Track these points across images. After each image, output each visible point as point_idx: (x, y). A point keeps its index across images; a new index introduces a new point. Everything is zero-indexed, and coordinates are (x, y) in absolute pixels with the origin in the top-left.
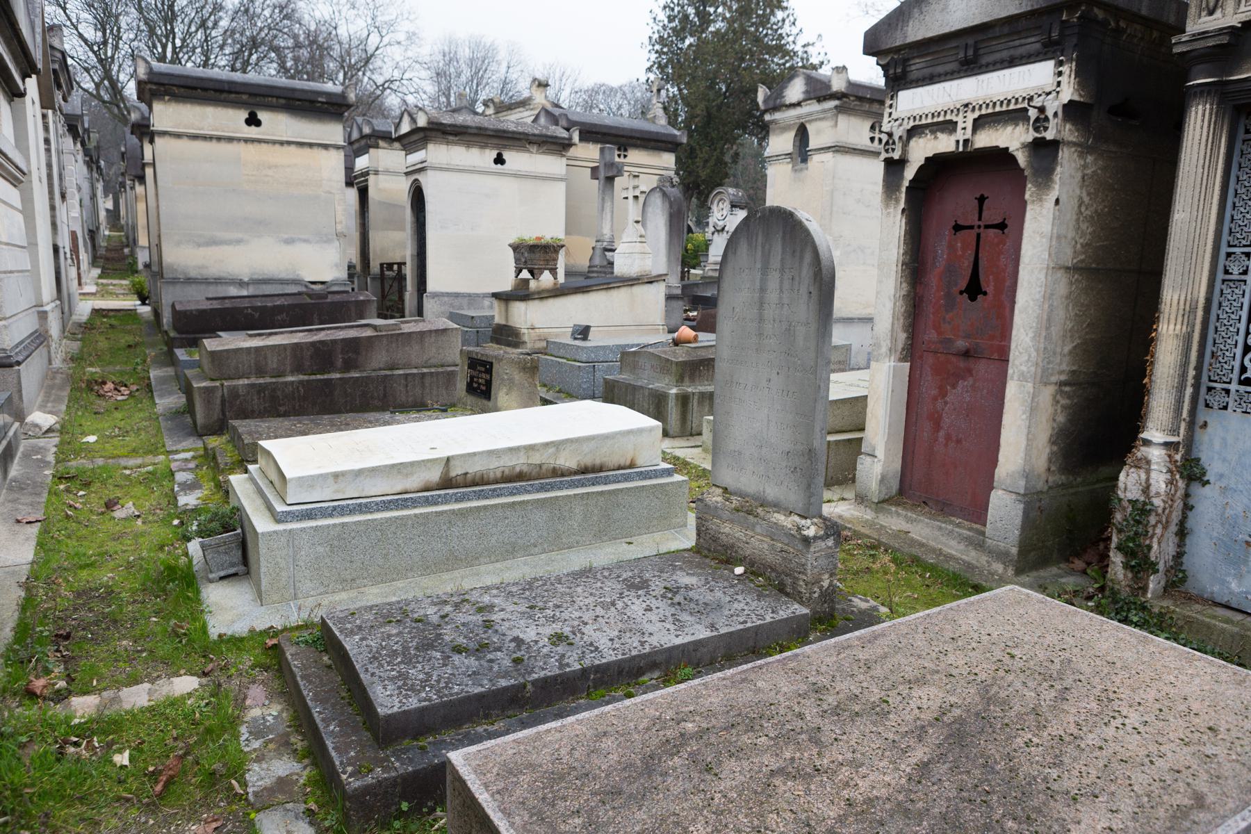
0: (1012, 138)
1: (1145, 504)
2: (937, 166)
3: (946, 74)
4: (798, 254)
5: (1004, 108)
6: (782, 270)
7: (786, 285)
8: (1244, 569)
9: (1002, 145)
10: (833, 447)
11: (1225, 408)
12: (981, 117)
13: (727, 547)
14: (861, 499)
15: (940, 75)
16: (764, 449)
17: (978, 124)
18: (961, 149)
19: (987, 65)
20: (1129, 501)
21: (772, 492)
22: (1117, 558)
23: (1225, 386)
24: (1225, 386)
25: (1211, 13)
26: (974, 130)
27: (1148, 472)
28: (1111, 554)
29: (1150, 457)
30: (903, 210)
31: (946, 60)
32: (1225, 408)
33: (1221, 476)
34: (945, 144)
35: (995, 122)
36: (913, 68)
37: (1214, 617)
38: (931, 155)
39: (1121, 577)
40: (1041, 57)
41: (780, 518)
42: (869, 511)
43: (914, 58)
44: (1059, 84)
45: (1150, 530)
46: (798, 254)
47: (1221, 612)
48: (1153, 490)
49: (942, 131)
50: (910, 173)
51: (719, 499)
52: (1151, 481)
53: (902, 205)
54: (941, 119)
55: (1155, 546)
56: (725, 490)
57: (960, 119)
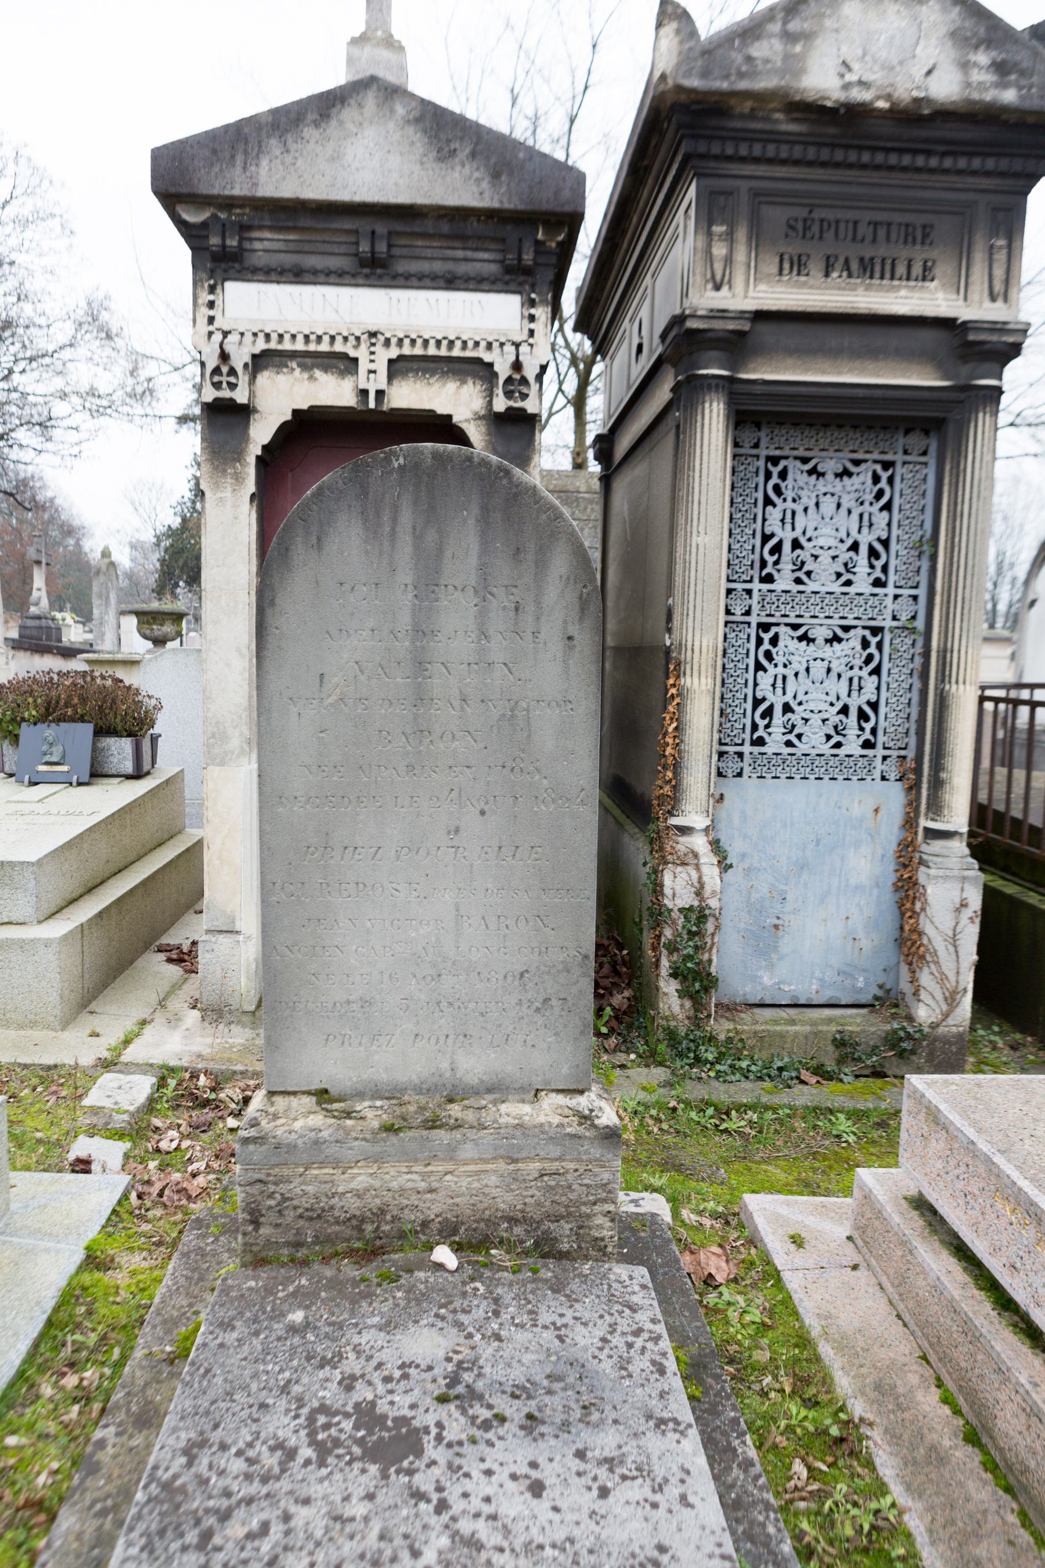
0: (459, 401)
1: (702, 909)
2: (308, 429)
3: (328, 273)
4: (530, 556)
5: (443, 352)
6: (483, 589)
7: (499, 621)
8: (774, 956)
9: (441, 410)
10: (86, 927)
11: (740, 775)
12: (401, 358)
13: (357, 1222)
14: (215, 1013)
15: (315, 272)
16: (448, 981)
17: (398, 367)
18: (372, 405)
19: (408, 277)
20: (681, 910)
21: (473, 1065)
22: (669, 988)
23: (738, 749)
24: (738, 749)
25: (717, 288)
26: (390, 378)
27: (697, 867)
28: (662, 984)
29: (696, 849)
30: (253, 496)
31: (329, 248)
32: (740, 775)
33: (744, 856)
34: (334, 392)
35: (425, 371)
36: (257, 245)
37: (776, 1022)
38: (305, 407)
40: (499, 285)
41: (513, 1111)
42: (236, 1029)
43: (261, 228)
44: (532, 333)
45: (708, 940)
46: (530, 556)
47: (768, 1013)
48: (707, 891)
49: (326, 369)
50: (261, 432)
51: (317, 1120)
52: (705, 879)
54: (324, 347)
55: (714, 958)
56: (322, 1095)
57: (362, 354)
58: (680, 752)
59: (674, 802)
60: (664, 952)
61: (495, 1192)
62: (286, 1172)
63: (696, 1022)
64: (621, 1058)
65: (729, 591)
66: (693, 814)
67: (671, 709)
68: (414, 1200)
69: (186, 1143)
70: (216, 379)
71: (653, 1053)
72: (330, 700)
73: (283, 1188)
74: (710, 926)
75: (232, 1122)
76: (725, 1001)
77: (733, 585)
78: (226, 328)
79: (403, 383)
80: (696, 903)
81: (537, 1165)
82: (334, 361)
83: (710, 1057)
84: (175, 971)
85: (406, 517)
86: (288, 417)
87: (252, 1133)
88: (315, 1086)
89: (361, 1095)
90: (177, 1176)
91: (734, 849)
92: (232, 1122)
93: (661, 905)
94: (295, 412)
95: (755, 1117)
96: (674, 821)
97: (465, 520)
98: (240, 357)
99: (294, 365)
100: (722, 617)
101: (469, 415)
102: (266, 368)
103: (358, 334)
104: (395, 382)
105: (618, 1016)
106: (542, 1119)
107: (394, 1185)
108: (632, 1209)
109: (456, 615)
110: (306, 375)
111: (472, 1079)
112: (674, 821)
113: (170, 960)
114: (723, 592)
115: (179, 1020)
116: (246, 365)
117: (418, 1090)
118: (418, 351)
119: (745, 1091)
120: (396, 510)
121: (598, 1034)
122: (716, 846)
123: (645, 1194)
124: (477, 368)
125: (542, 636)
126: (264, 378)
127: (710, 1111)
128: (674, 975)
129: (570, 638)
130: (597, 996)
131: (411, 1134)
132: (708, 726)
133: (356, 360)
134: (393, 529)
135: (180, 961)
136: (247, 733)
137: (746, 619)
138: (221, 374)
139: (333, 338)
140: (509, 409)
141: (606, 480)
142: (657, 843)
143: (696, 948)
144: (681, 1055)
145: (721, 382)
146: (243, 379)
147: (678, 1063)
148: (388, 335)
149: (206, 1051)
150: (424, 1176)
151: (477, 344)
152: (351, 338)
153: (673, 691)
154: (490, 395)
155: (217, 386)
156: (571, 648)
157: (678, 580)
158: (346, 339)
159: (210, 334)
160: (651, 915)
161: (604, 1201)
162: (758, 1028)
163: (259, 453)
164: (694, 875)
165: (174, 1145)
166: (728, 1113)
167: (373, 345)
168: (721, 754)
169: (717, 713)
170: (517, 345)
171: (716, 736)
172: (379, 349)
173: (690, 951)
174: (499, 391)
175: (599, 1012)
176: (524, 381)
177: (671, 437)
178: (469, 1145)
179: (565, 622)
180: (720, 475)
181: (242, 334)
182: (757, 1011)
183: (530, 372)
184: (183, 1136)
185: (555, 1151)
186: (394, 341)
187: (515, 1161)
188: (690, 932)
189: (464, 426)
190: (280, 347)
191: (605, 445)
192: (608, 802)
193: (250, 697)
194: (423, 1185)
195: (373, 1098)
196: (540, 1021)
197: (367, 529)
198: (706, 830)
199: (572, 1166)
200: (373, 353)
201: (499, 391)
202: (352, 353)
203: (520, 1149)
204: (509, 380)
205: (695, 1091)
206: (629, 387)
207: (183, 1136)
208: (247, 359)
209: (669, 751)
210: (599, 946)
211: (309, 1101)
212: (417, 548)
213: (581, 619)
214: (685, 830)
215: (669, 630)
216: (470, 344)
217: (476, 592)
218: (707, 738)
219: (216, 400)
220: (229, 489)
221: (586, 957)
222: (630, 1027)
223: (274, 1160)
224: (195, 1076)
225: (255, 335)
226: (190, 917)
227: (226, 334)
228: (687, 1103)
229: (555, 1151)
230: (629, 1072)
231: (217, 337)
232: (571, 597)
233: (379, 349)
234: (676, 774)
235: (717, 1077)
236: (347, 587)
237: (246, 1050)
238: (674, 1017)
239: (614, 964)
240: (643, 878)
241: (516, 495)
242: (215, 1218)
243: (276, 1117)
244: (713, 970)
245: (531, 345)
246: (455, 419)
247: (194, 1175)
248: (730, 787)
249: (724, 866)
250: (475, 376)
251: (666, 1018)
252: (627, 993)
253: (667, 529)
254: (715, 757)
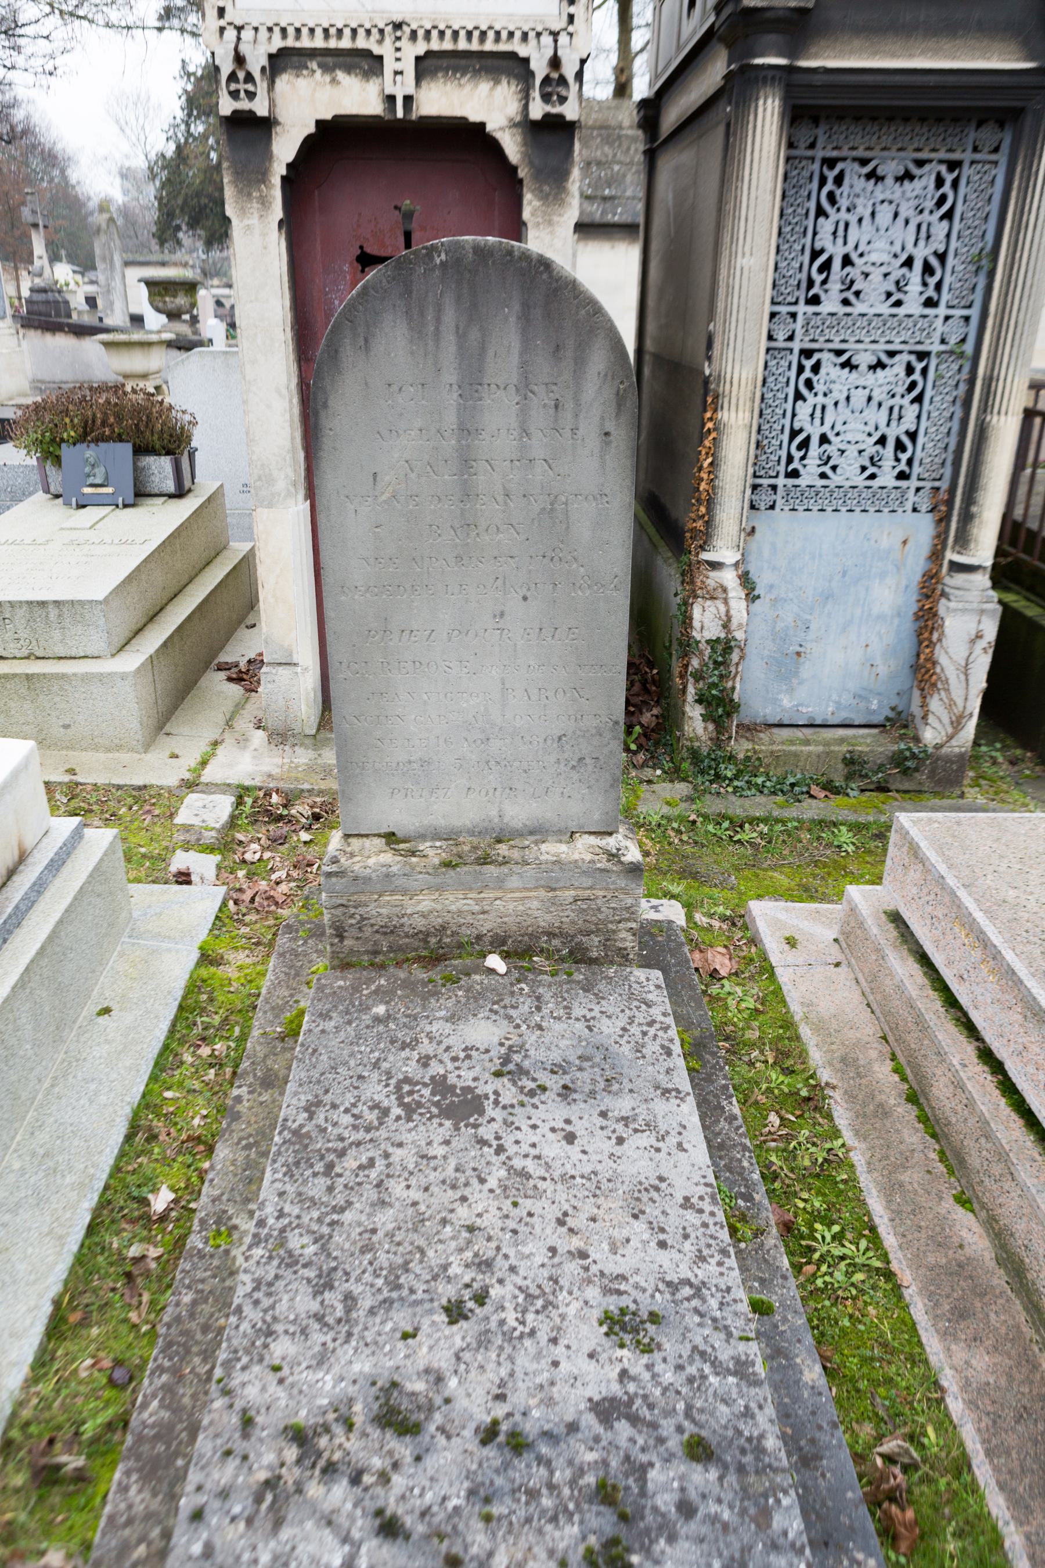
1: (728, 641)
2: (335, 141)
4: (569, 353)
5: (475, 46)
6: (525, 388)
7: (539, 418)
8: (795, 681)
9: (474, 117)
11: (772, 507)
12: (429, 54)
13: (424, 936)
14: (281, 737)
18: (400, 114)
20: (708, 642)
21: (518, 812)
22: (694, 712)
23: (772, 481)
24: (772, 481)
27: (726, 601)
28: (688, 709)
29: (725, 583)
30: (281, 222)
33: (771, 587)
34: (358, 98)
35: (455, 70)
37: (792, 742)
38: (328, 116)
39: (700, 731)
41: (552, 849)
44: (571, 18)
45: (733, 669)
46: (569, 353)
47: (786, 733)
49: (349, 69)
50: (285, 148)
51: (387, 857)
52: (732, 612)
53: (277, 212)
54: (346, 43)
56: (390, 838)
57: (385, 50)
58: (714, 488)
59: (706, 538)
60: (691, 680)
61: (536, 913)
62: (363, 898)
63: (717, 743)
64: (648, 773)
65: (773, 315)
66: (724, 550)
67: (707, 443)
68: (470, 919)
69: (267, 855)
70: (233, 86)
71: (677, 770)
72: (384, 498)
73: (361, 910)
74: (735, 657)
75: (305, 836)
76: (746, 722)
77: (777, 308)
78: (239, 22)
79: (432, 85)
80: (723, 635)
81: (572, 893)
82: (357, 60)
83: (729, 774)
84: (235, 690)
85: (449, 316)
86: (311, 129)
87: (334, 868)
88: (384, 830)
89: (423, 837)
90: (263, 885)
91: (763, 580)
92: (305, 836)
93: (690, 637)
94: (319, 123)
95: (766, 830)
96: (705, 556)
97: (506, 318)
98: (257, 61)
99: (314, 65)
100: (764, 343)
101: (504, 122)
102: (284, 70)
103: (381, 25)
104: (424, 84)
105: (646, 734)
106: (576, 856)
107: (453, 908)
108: (653, 916)
109: (499, 411)
110: (327, 78)
111: (517, 824)
112: (705, 556)
113: (230, 679)
114: (766, 317)
115: (246, 740)
116: (263, 69)
117: (471, 833)
118: (447, 45)
119: (758, 805)
120: (439, 310)
121: (627, 750)
122: (746, 580)
123: (664, 901)
124: (511, 63)
125: (580, 433)
126: (284, 82)
127: (726, 824)
128: (699, 701)
129: (607, 434)
130: (628, 713)
131: (466, 869)
132: (742, 465)
133: (380, 58)
134: (437, 329)
135: (238, 680)
136: (292, 475)
137: (789, 344)
138: (237, 81)
139: (354, 32)
140: (547, 116)
141: (651, 156)
142: (688, 575)
143: (721, 676)
144: (702, 772)
145: (778, 74)
146: (262, 86)
147: (700, 779)
148: (414, 26)
149: (276, 771)
150: (478, 901)
151: (511, 34)
152: (375, 31)
153: (710, 425)
154: (526, 98)
155: (235, 95)
156: (608, 444)
157: (720, 305)
158: (368, 32)
159: (222, 30)
160: (680, 644)
161: (628, 920)
162: (775, 748)
163: (284, 172)
164: (722, 609)
165: (257, 856)
166: (741, 826)
167: (398, 39)
168: (755, 487)
169: (753, 446)
170: (555, 34)
171: (751, 471)
172: (404, 43)
173: (715, 679)
174: (536, 94)
175: (629, 731)
176: (562, 81)
177: (721, 129)
178: (515, 878)
179: (602, 418)
180: (770, 186)
181: (256, 29)
182: (775, 730)
183: (569, 70)
184: (264, 849)
185: (588, 882)
186: (421, 33)
187: (554, 890)
188: (715, 662)
189: (498, 135)
190: (298, 45)
191: (650, 111)
192: (642, 515)
193: (293, 438)
194: (477, 908)
195: (433, 839)
196: (575, 776)
197: (411, 329)
198: (736, 565)
199: (601, 893)
200: (398, 49)
201: (536, 94)
202: (376, 50)
203: (558, 880)
204: (547, 80)
205: (713, 806)
206: (679, 48)
207: (264, 849)
208: (264, 61)
209: (703, 486)
210: (630, 665)
211: (380, 842)
212: (460, 347)
213: (618, 415)
214: (715, 566)
215: (709, 358)
216: (504, 35)
217: (517, 390)
218: (741, 473)
219: (235, 112)
220: (256, 215)
221: (616, 723)
222: (657, 744)
223: (352, 890)
224: (268, 794)
225: (270, 29)
226: (242, 633)
227: (239, 29)
228: (706, 817)
229: (588, 882)
230: (655, 787)
231: (231, 34)
232: (609, 393)
233: (404, 43)
234: (710, 509)
235: (734, 793)
236: (395, 388)
237: (311, 769)
238: (698, 739)
239: (644, 683)
240: (674, 610)
241: (556, 290)
242: (302, 923)
243: (352, 855)
244: (736, 697)
245: (571, 35)
246: (489, 128)
247: (277, 883)
248: (763, 521)
249: (752, 597)
250: (510, 74)
251: (691, 740)
252: (655, 711)
253: (711, 239)
254: (749, 491)
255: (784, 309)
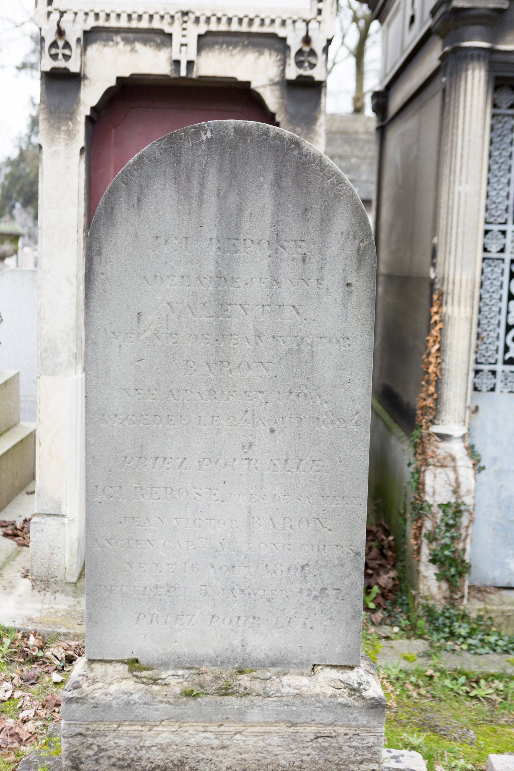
0: (258, 71)
1: (458, 506)
2: (130, 94)
4: (316, 215)
5: (244, 28)
6: (276, 243)
9: (242, 78)
11: (493, 390)
12: (209, 33)
14: (44, 583)
17: (205, 41)
20: (440, 506)
21: (261, 643)
23: (492, 367)
26: (200, 49)
27: (455, 469)
30: (82, 149)
32: (493, 390)
33: (495, 459)
34: (152, 62)
35: (229, 44)
39: (434, 590)
41: (294, 682)
44: (320, 12)
45: (463, 531)
46: (316, 215)
48: (463, 490)
49: (145, 42)
50: (90, 96)
51: (129, 685)
52: (461, 479)
53: (80, 141)
54: (144, 24)
55: (468, 547)
56: (133, 664)
57: (175, 30)
58: (441, 370)
59: (435, 413)
60: (425, 541)
61: (277, 750)
62: (102, 727)
63: (451, 602)
64: (386, 630)
65: (486, 232)
66: (451, 422)
67: (434, 332)
68: (208, 754)
69: (18, 694)
70: (54, 51)
71: (413, 627)
72: (146, 335)
73: (99, 741)
74: (465, 520)
75: (56, 677)
76: (477, 584)
77: (489, 227)
78: (62, 9)
79: (210, 54)
80: (453, 500)
81: (314, 729)
82: (152, 36)
83: (463, 632)
84: (10, 544)
85: (213, 182)
86: (113, 83)
87: (75, 694)
88: (127, 656)
89: (165, 665)
90: (10, 722)
91: (487, 454)
92: (56, 677)
93: (423, 501)
94: (119, 79)
95: (501, 686)
96: (434, 429)
97: (261, 185)
98: (74, 33)
99: (118, 38)
100: (480, 255)
101: (265, 81)
102: (95, 41)
103: (172, 13)
104: (203, 53)
105: (384, 594)
106: (318, 690)
107: (192, 741)
108: (393, 764)
109: (253, 264)
110: (128, 48)
111: (259, 654)
112: (434, 429)
113: (6, 535)
114: (481, 233)
115: (13, 587)
116: (78, 40)
117: (214, 662)
118: (223, 27)
119: (492, 663)
120: (203, 176)
121: (367, 609)
122: (471, 450)
123: (405, 752)
124: (272, 41)
125: (325, 283)
126: (93, 50)
127: (462, 680)
128: (433, 561)
129: (348, 285)
130: (367, 576)
131: (207, 699)
132: (466, 348)
133: (170, 35)
134: (201, 192)
135: (15, 535)
136: (74, 349)
137: (501, 255)
138: (57, 47)
139: (151, 17)
140: (300, 77)
141: (382, 131)
142: (420, 447)
143: (453, 538)
144: (437, 630)
145: (483, 53)
146: (76, 51)
147: (435, 637)
148: (198, 14)
149: (35, 615)
150: (218, 735)
151: (273, 21)
152: (167, 17)
153: (436, 318)
154: (284, 64)
155: (54, 57)
156: (350, 293)
157: (442, 222)
158: (162, 17)
159: (49, 13)
160: (414, 509)
161: (370, 761)
162: (506, 608)
163: (88, 113)
164: (452, 476)
165: (8, 695)
166: (477, 682)
167: (185, 22)
168: (477, 372)
169: (474, 336)
170: (307, 23)
171: (473, 357)
172: (190, 25)
173: (447, 541)
174: (291, 61)
175: (368, 589)
176: (312, 53)
177: (438, 99)
178: (256, 710)
179: (345, 271)
180: (479, 132)
181: (76, 14)
182: (505, 593)
183: (318, 45)
184: (15, 688)
185: (329, 718)
186: (203, 19)
187: (294, 725)
188: (447, 525)
189: (261, 91)
190: (107, 25)
191: (381, 100)
192: (379, 407)
193: (77, 318)
194: (216, 743)
195: (176, 668)
196: (318, 606)
197: (179, 192)
198: (463, 437)
199: (343, 730)
200: (184, 29)
201: (291, 61)
202: (167, 30)
203: (299, 715)
204: (300, 52)
205: (448, 662)
206: (403, 52)
207: (15, 688)
208: (80, 35)
209: (432, 369)
210: (369, 532)
211: (123, 669)
212: (220, 208)
213: (358, 269)
214: (444, 437)
215: (434, 265)
216: (267, 21)
217: (270, 245)
218: (465, 358)
219: (53, 69)
220: (63, 143)
221: (358, 554)
222: (394, 603)
223: (92, 718)
224: (26, 636)
225: (86, 14)
226: (23, 497)
227: (62, 14)
228: (442, 672)
229: (329, 718)
230: (393, 643)
231: (55, 16)
232: (350, 250)
233: (190, 25)
234: (438, 388)
235: (469, 650)
236: (161, 240)
237: (69, 615)
238: (433, 597)
239: (381, 549)
240: (408, 477)
241: (305, 164)
242: (42, 760)
243: (94, 681)
244: (467, 558)
245: (320, 22)
246: (253, 86)
247: (24, 722)
248: (484, 400)
249: (478, 468)
250: (271, 48)
251: (425, 598)
252: (392, 574)
253: (433, 176)
254: (472, 374)
255: (495, 228)
